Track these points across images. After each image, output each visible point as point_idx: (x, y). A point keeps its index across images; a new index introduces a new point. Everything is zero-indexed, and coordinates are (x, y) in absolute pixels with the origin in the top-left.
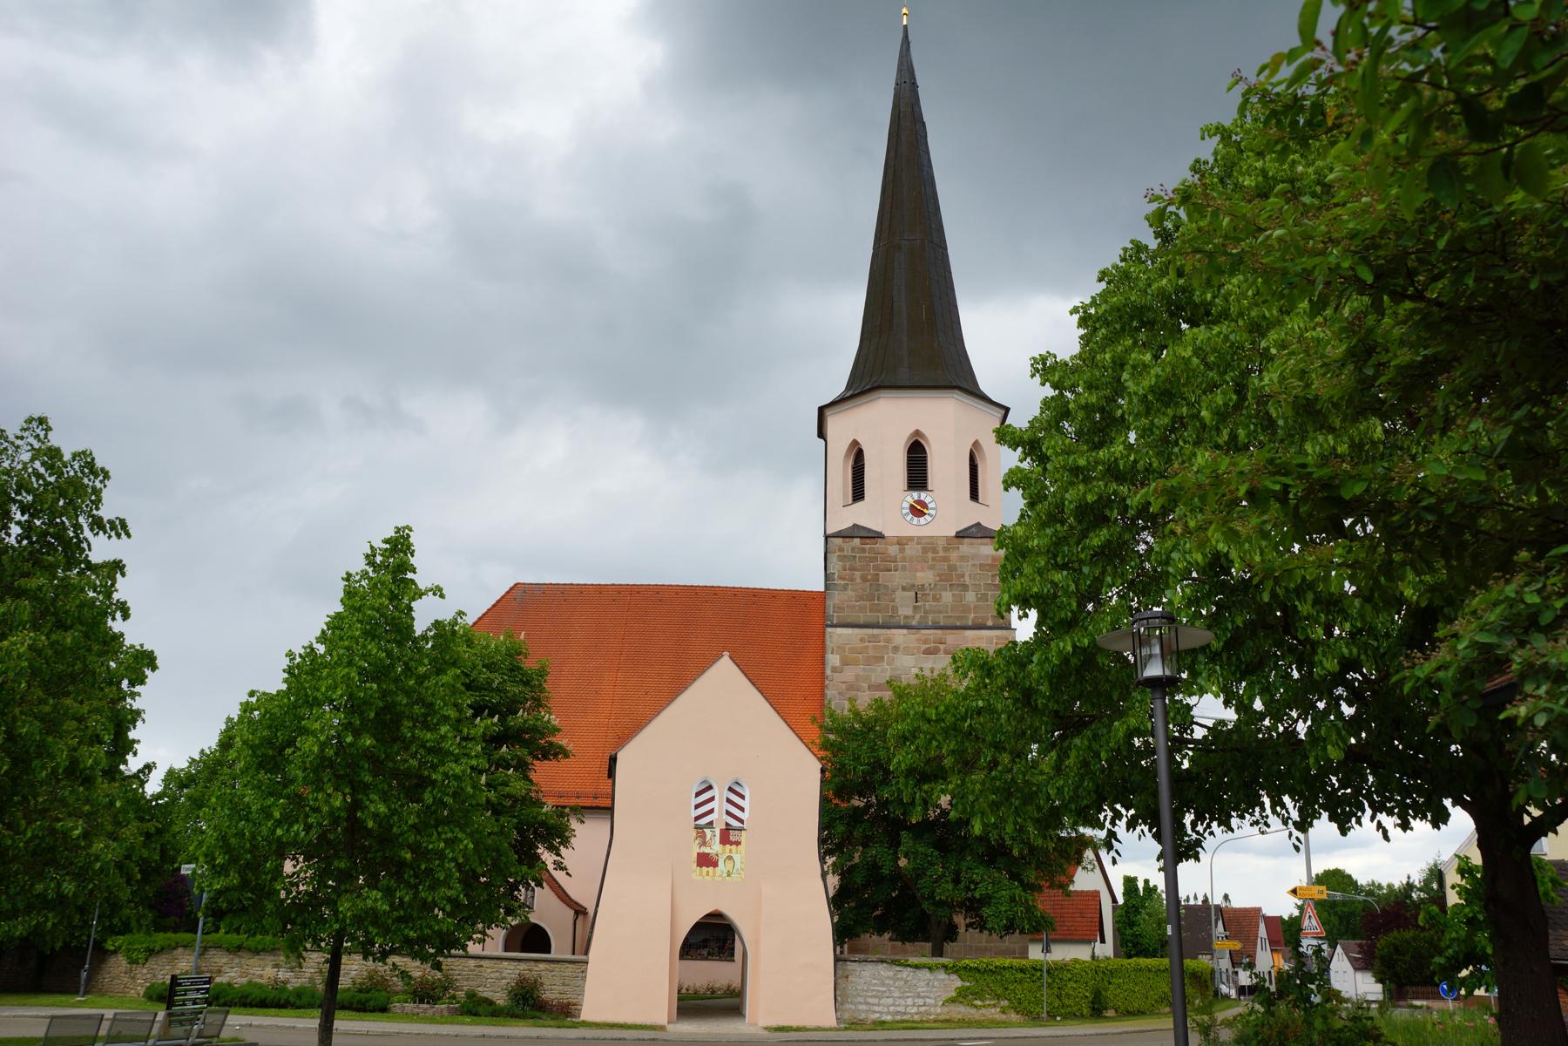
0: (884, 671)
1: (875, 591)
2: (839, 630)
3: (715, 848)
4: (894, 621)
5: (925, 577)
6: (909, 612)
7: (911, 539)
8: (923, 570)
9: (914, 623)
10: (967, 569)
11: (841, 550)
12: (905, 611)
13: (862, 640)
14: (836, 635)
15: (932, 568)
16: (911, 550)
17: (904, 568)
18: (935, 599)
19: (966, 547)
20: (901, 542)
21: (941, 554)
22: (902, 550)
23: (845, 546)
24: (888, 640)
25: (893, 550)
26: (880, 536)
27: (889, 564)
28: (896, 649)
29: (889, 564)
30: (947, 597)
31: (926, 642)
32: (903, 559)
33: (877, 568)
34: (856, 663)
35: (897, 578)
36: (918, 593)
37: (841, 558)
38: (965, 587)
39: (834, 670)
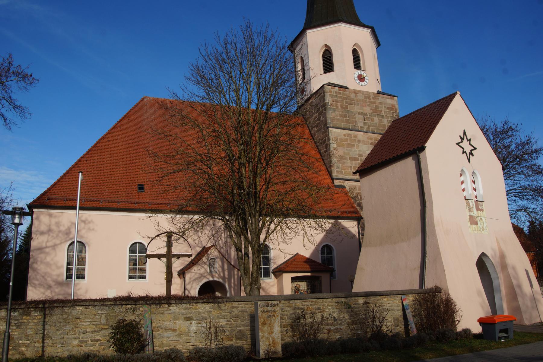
0: (355, 151)
1: (347, 114)
2: (334, 130)
3: (475, 213)
4: (357, 128)
5: (367, 110)
6: (362, 125)
7: (359, 91)
8: (365, 106)
9: (365, 130)
10: (383, 109)
11: (331, 92)
12: (360, 124)
13: (345, 135)
14: (334, 132)
15: (369, 106)
16: (360, 97)
17: (358, 104)
18: (372, 120)
19: (381, 98)
20: (356, 92)
21: (372, 100)
22: (356, 96)
23: (332, 90)
24: (356, 137)
25: (353, 96)
26: (346, 88)
27: (351, 102)
28: (359, 141)
29: (351, 102)
30: (376, 120)
31: (371, 139)
32: (357, 100)
33: (346, 102)
34: (343, 146)
35: (356, 109)
36: (365, 117)
37: (332, 96)
38: (383, 117)
39: (335, 149)
